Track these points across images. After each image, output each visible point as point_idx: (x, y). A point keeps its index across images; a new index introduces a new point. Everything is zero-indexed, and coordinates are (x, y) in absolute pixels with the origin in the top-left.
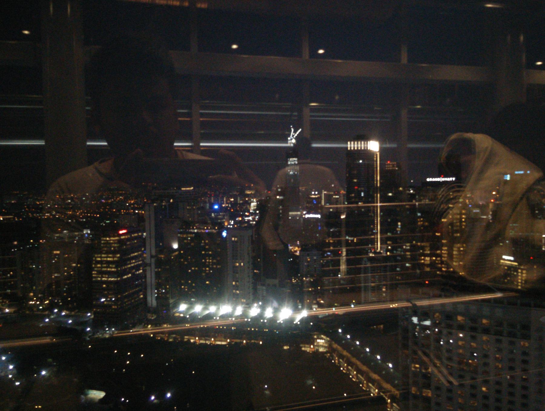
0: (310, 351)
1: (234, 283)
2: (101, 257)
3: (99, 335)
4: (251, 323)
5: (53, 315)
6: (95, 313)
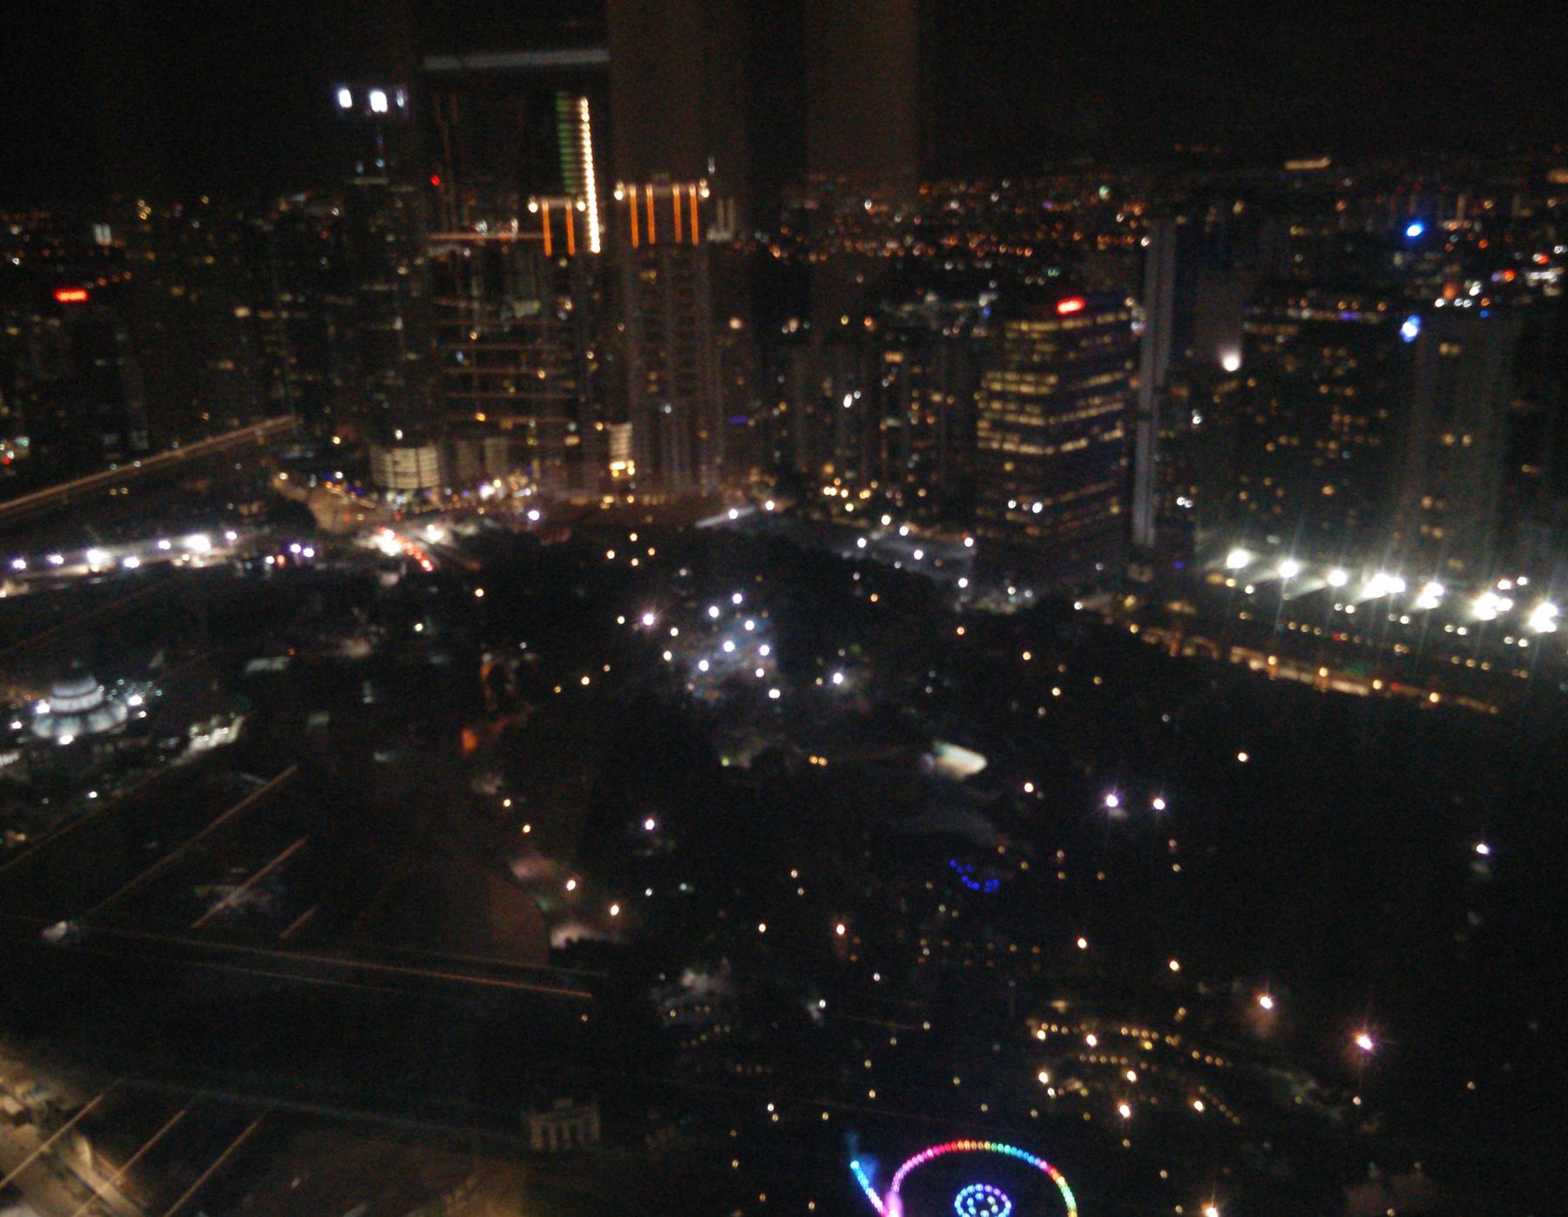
2: (1003, 381)
3: (988, 603)
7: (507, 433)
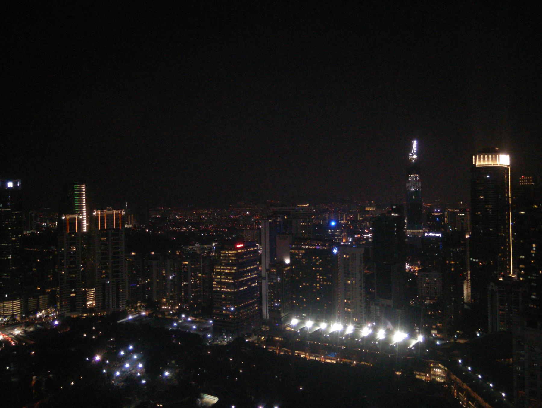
1: (345, 301)
2: (220, 269)
5: (181, 320)
6: (215, 321)
7: (48, 293)
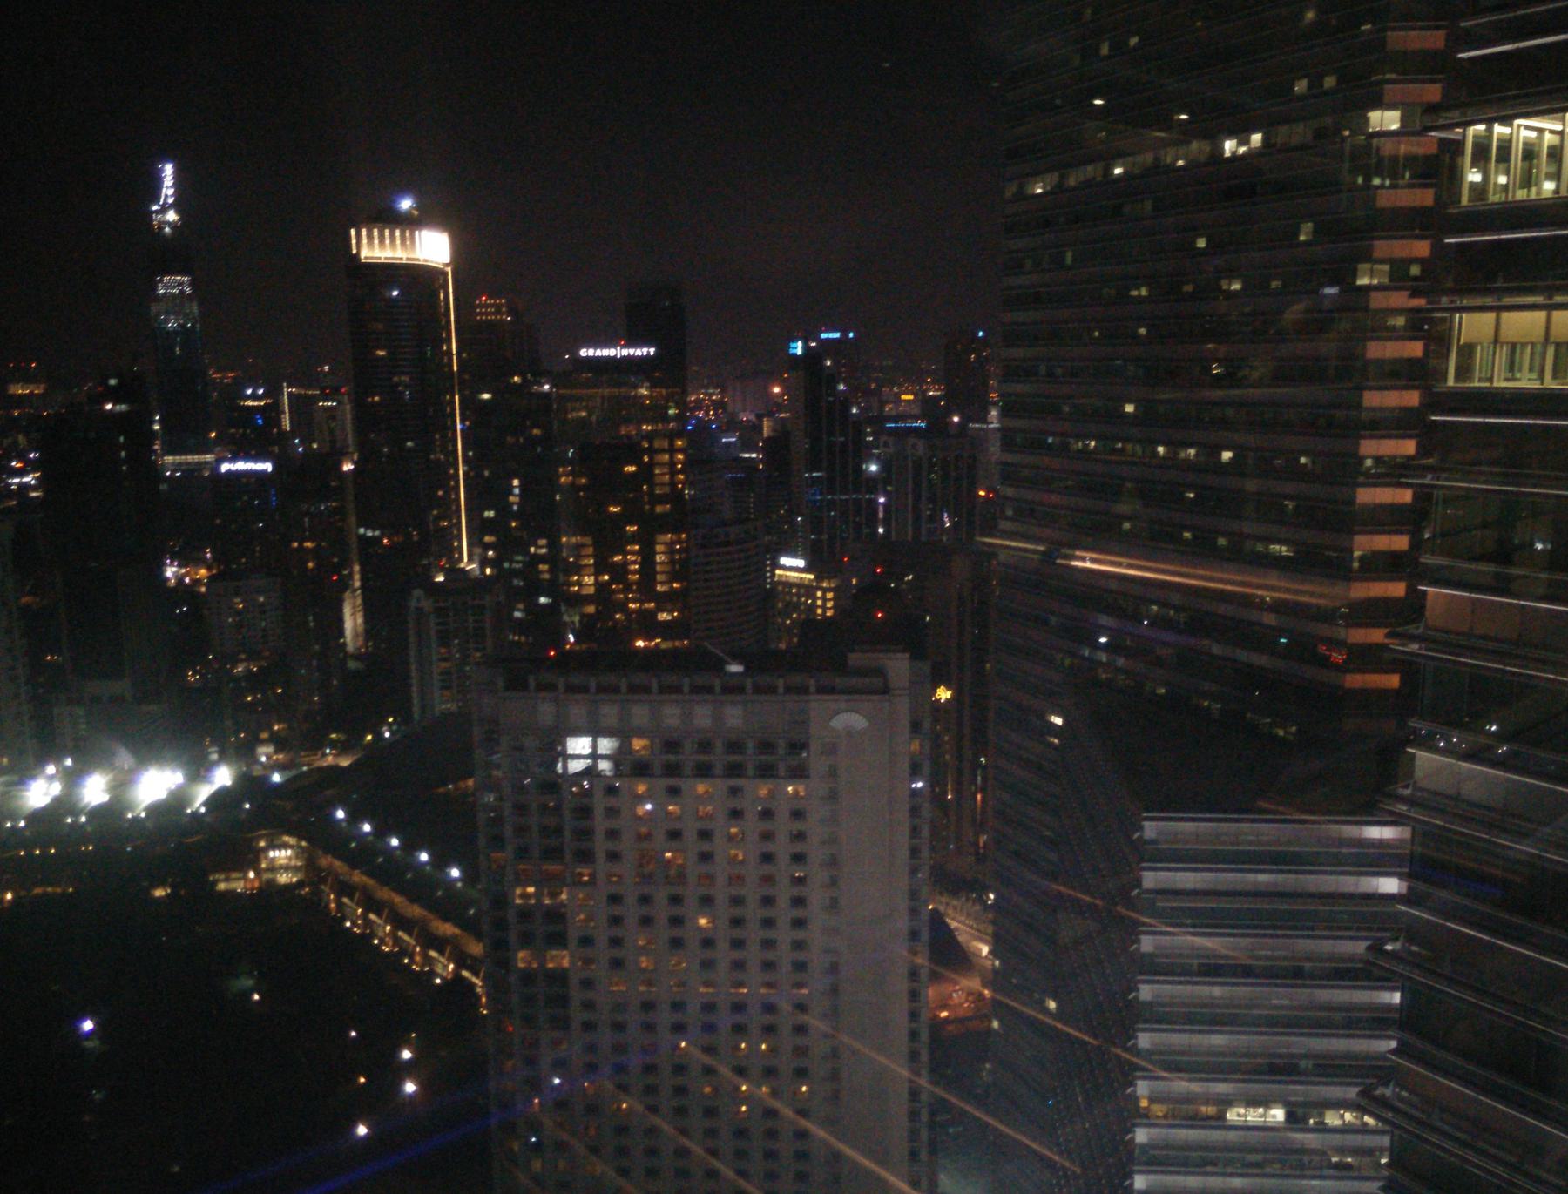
0: (245, 888)
4: (28, 833)
